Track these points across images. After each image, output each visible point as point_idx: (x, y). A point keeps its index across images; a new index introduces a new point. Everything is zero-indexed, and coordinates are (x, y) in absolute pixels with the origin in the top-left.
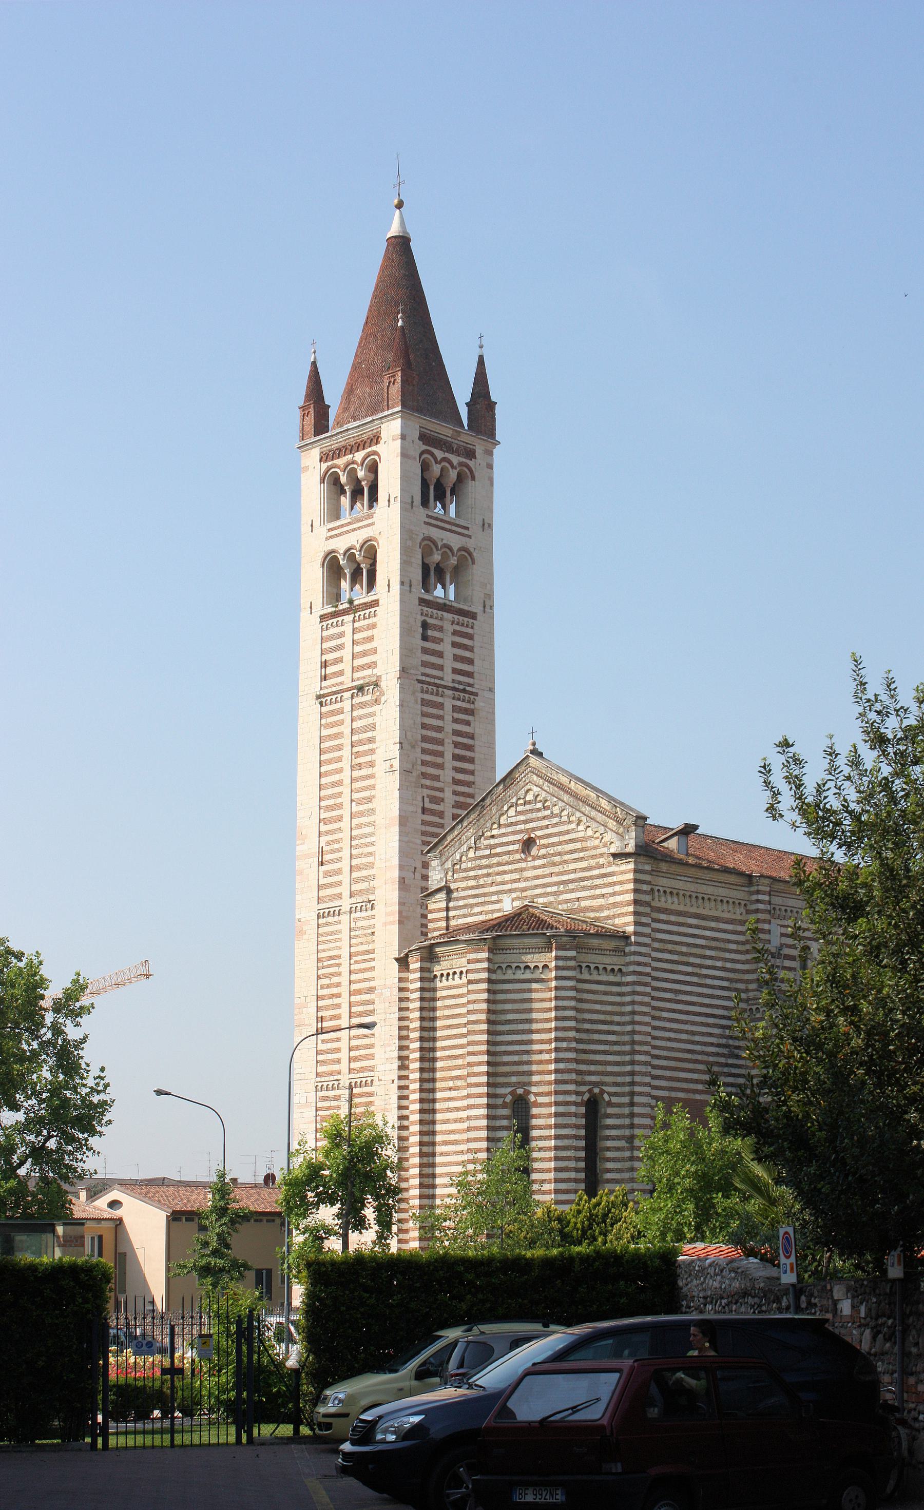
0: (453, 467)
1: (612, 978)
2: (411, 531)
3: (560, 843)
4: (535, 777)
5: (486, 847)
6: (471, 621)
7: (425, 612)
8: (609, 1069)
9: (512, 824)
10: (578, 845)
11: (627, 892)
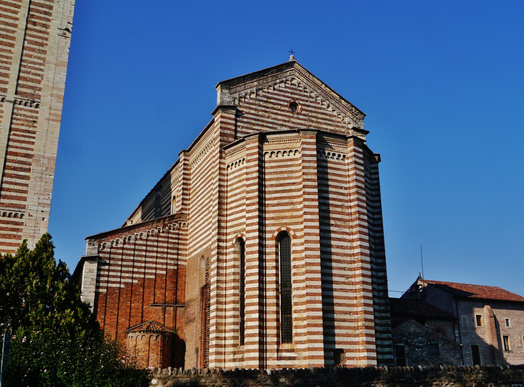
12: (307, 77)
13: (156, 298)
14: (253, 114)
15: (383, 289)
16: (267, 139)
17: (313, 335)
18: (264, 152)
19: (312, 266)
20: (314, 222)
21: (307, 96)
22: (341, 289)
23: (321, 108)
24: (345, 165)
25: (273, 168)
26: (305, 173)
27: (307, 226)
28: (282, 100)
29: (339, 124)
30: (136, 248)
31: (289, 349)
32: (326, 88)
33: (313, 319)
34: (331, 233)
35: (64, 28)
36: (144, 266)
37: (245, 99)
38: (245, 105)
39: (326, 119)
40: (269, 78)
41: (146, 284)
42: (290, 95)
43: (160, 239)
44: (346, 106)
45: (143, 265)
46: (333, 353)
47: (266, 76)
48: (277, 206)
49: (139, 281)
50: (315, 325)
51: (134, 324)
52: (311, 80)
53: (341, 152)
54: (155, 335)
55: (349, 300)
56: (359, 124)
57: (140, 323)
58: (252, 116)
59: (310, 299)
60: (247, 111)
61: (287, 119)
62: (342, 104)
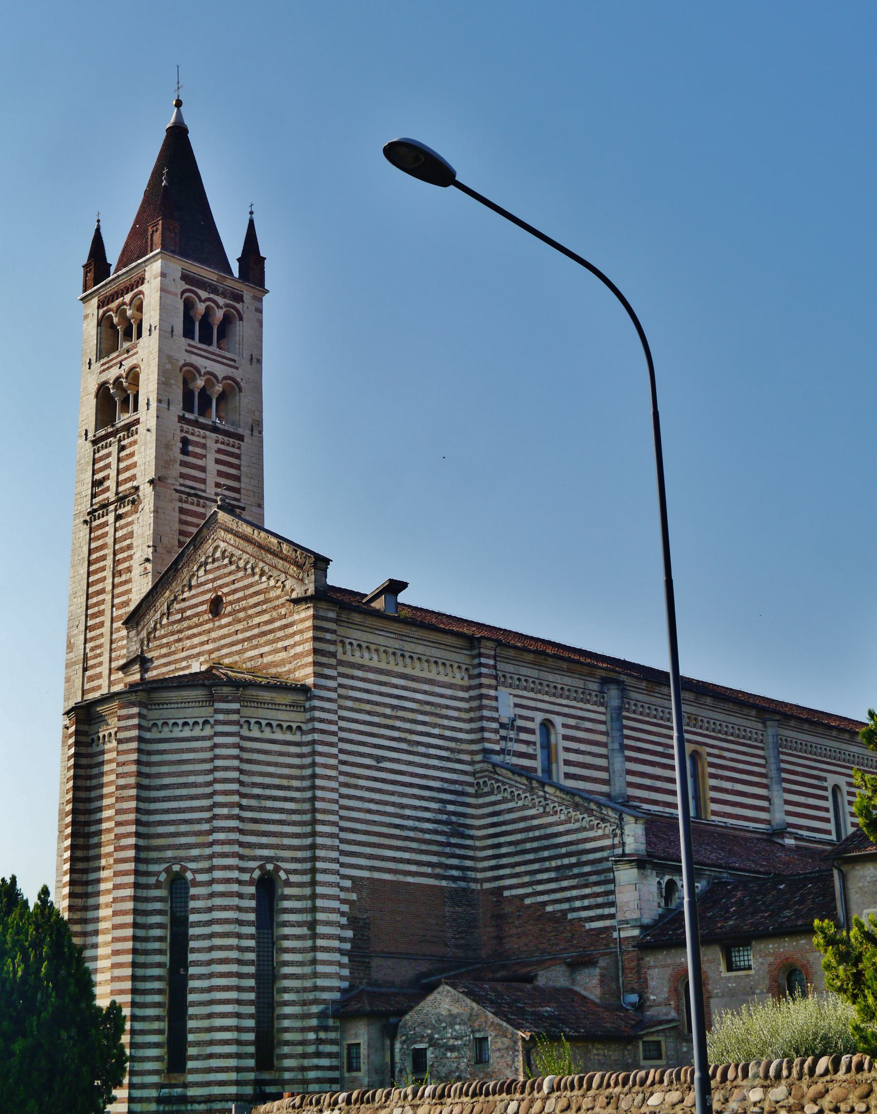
0: (219, 307)
1: (289, 737)
2: (170, 358)
3: (245, 598)
4: (222, 532)
5: (178, 612)
6: (237, 442)
7: (185, 429)
8: (287, 841)
9: (202, 584)
10: (261, 597)
11: (306, 641)
35: (143, 559)
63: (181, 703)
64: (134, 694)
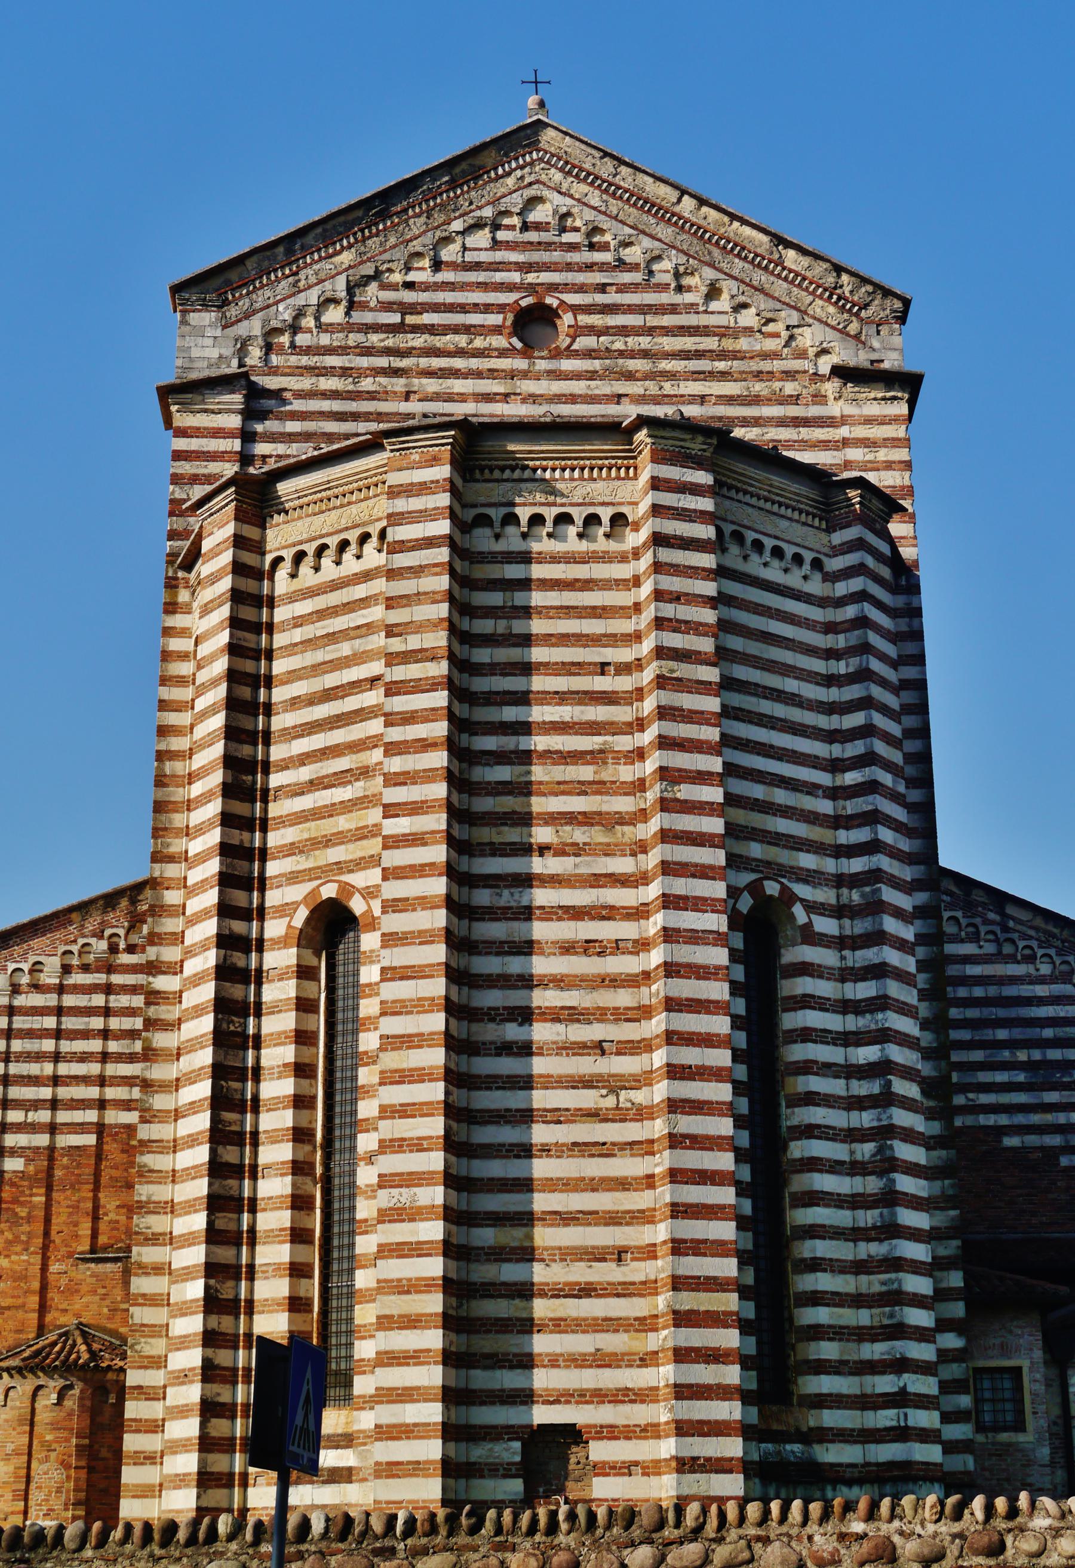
12: (604, 181)
13: (102, 1226)
14: (334, 395)
15: (875, 1124)
16: (279, 497)
17: (399, 1365)
18: (269, 558)
19: (409, 1048)
20: (425, 844)
21: (602, 267)
22: (575, 1144)
23: (673, 309)
24: (623, 558)
25: (301, 625)
26: (397, 625)
27: (396, 868)
28: (476, 308)
29: (766, 366)
30: (15, 1026)
31: (340, 1431)
32: (705, 209)
33: (399, 1293)
34: (531, 886)
36: (49, 1097)
37: (294, 333)
38: (293, 360)
39: (699, 355)
40: (411, 221)
41: (58, 1173)
42: (515, 277)
43: (117, 979)
44: (808, 274)
45: (46, 1093)
46: (517, 1445)
47: (397, 213)
48: (310, 791)
49: (29, 1160)
50: (409, 1321)
51: (11, 1342)
52: (626, 191)
53: (603, 504)
54: (55, 1384)
55: (618, 1195)
56: (876, 344)
57: (31, 1336)
58: (326, 405)
59: (395, 1200)
60: (305, 383)
61: (496, 387)
62: (784, 268)
63: (766, 500)
64: (700, 439)
